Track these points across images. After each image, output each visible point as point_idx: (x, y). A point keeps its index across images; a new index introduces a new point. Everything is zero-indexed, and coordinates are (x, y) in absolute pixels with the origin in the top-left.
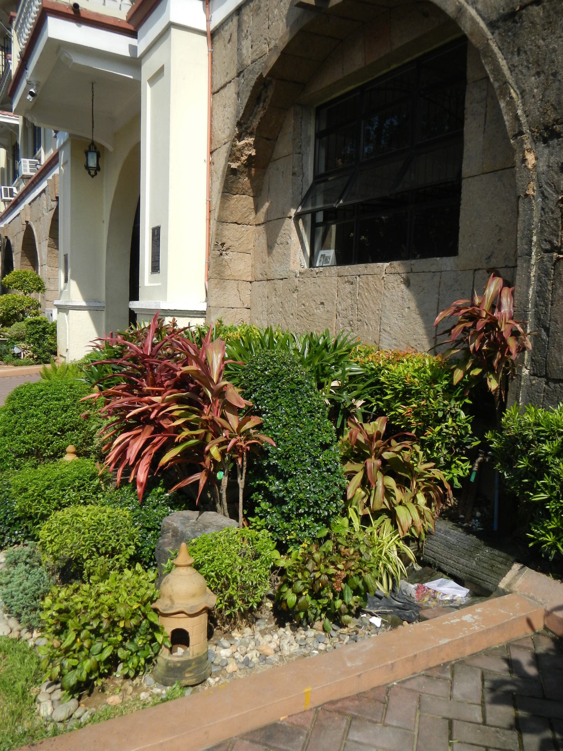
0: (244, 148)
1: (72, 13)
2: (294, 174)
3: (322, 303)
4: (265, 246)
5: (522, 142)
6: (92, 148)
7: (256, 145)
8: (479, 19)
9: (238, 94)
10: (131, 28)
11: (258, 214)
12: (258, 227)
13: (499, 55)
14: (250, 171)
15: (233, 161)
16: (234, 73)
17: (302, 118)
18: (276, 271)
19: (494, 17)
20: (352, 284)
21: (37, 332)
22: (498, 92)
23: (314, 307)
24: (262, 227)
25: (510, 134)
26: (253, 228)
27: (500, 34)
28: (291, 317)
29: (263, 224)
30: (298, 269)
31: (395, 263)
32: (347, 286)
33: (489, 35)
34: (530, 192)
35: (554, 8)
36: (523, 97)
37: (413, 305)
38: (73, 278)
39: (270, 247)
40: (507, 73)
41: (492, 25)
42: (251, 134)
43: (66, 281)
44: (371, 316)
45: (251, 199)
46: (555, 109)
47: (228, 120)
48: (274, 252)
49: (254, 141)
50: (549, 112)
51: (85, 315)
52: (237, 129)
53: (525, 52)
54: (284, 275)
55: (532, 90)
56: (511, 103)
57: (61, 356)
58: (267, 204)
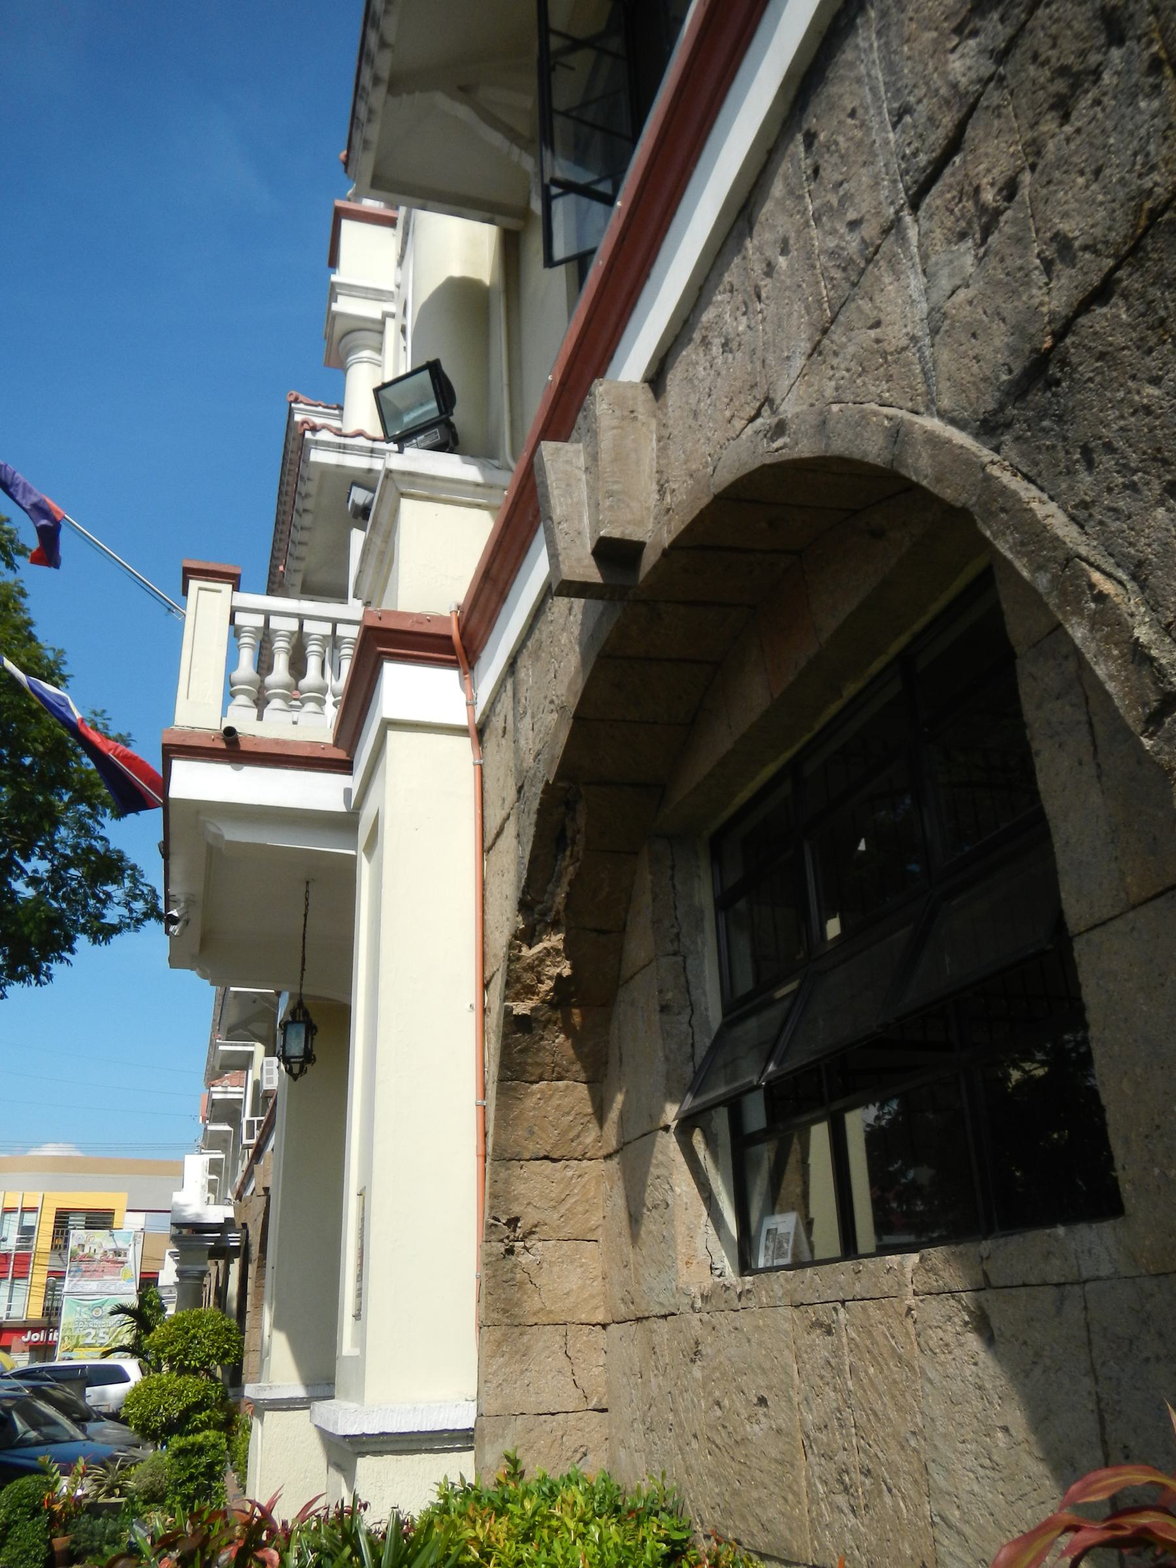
0: (541, 961)
1: (223, 746)
2: (664, 1009)
3: (762, 1401)
4: (623, 1215)
7: (570, 951)
10: (341, 754)
11: (605, 1128)
13: (1027, 492)
14: (567, 1017)
15: (517, 997)
17: (673, 867)
18: (651, 1289)
19: (989, 403)
20: (829, 1332)
21: (191, 1478)
25: (1133, 718)
26: (599, 1166)
30: (696, 1280)
31: (936, 1255)
32: (817, 1336)
33: (986, 454)
36: (1143, 586)
37: (1016, 1417)
39: (634, 1220)
42: (555, 926)
45: (582, 1090)
49: (565, 940)
52: (520, 918)
53: (1109, 448)
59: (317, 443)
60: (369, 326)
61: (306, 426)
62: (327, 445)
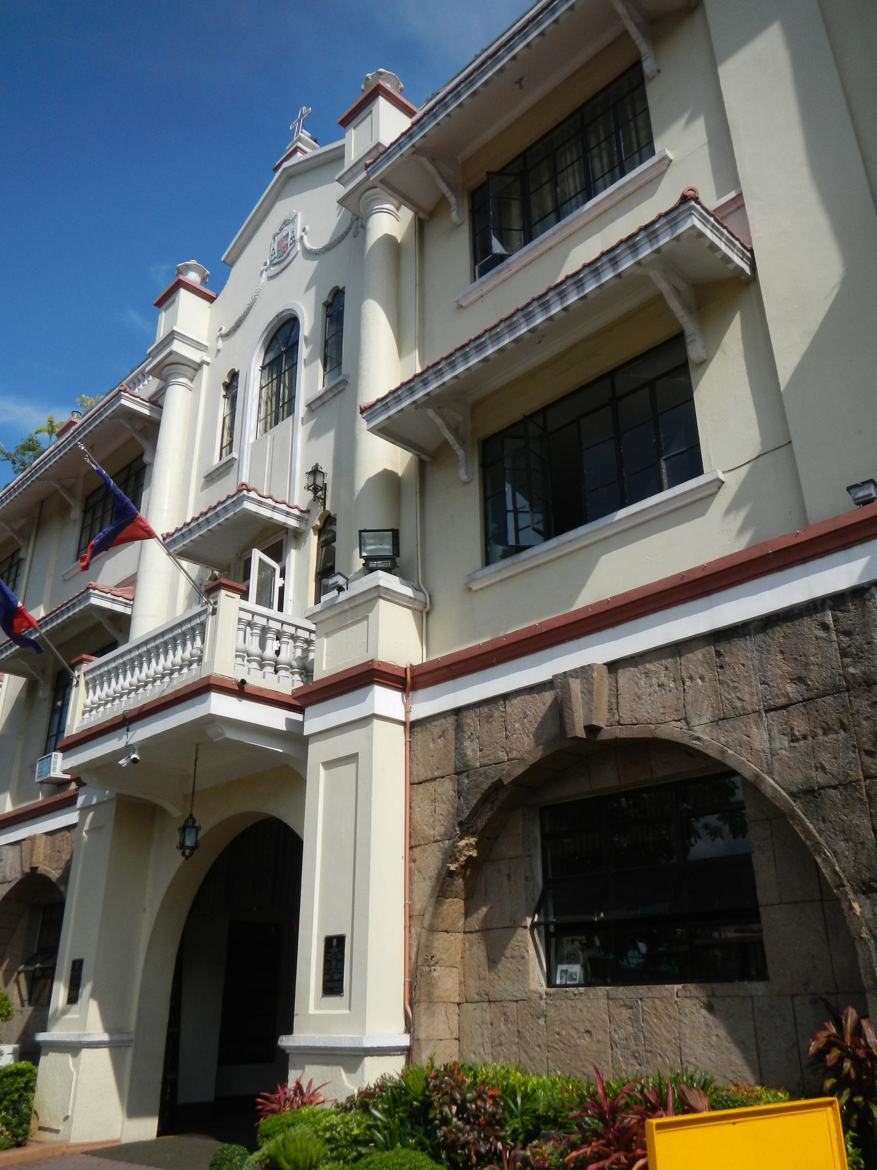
1: (237, 688)
3: (588, 1032)
5: (846, 894)
6: (190, 823)
7: (477, 846)
8: (779, 788)
9: (459, 793)
11: (469, 920)
12: (469, 935)
14: (465, 871)
16: (451, 769)
19: (794, 789)
20: (631, 1008)
22: (812, 849)
23: (575, 1036)
24: (479, 934)
25: (832, 884)
27: (802, 803)
28: (538, 1049)
29: (477, 931)
33: (794, 804)
34: (864, 935)
35: (850, 795)
38: (93, 996)
39: (493, 961)
40: (817, 835)
41: (791, 794)
42: (473, 835)
43: (73, 999)
44: (665, 1045)
46: (869, 870)
47: (441, 817)
48: (500, 967)
49: (477, 843)
50: (864, 871)
51: (104, 1054)
52: (457, 829)
53: (830, 822)
54: (519, 995)
55: (843, 852)
56: (826, 859)
57: (41, 1128)
58: (484, 910)
59: (249, 498)
60: (189, 364)
61: (244, 487)
62: (253, 500)
